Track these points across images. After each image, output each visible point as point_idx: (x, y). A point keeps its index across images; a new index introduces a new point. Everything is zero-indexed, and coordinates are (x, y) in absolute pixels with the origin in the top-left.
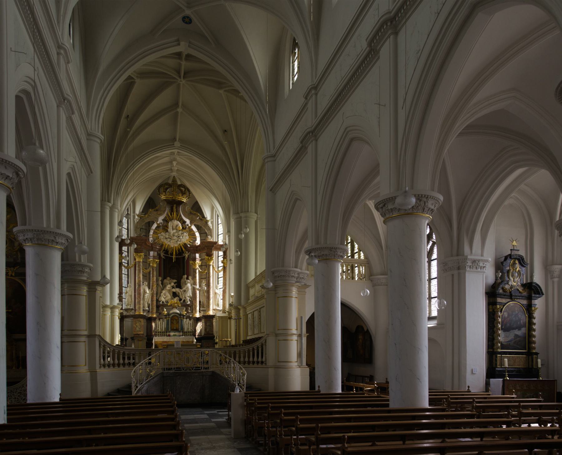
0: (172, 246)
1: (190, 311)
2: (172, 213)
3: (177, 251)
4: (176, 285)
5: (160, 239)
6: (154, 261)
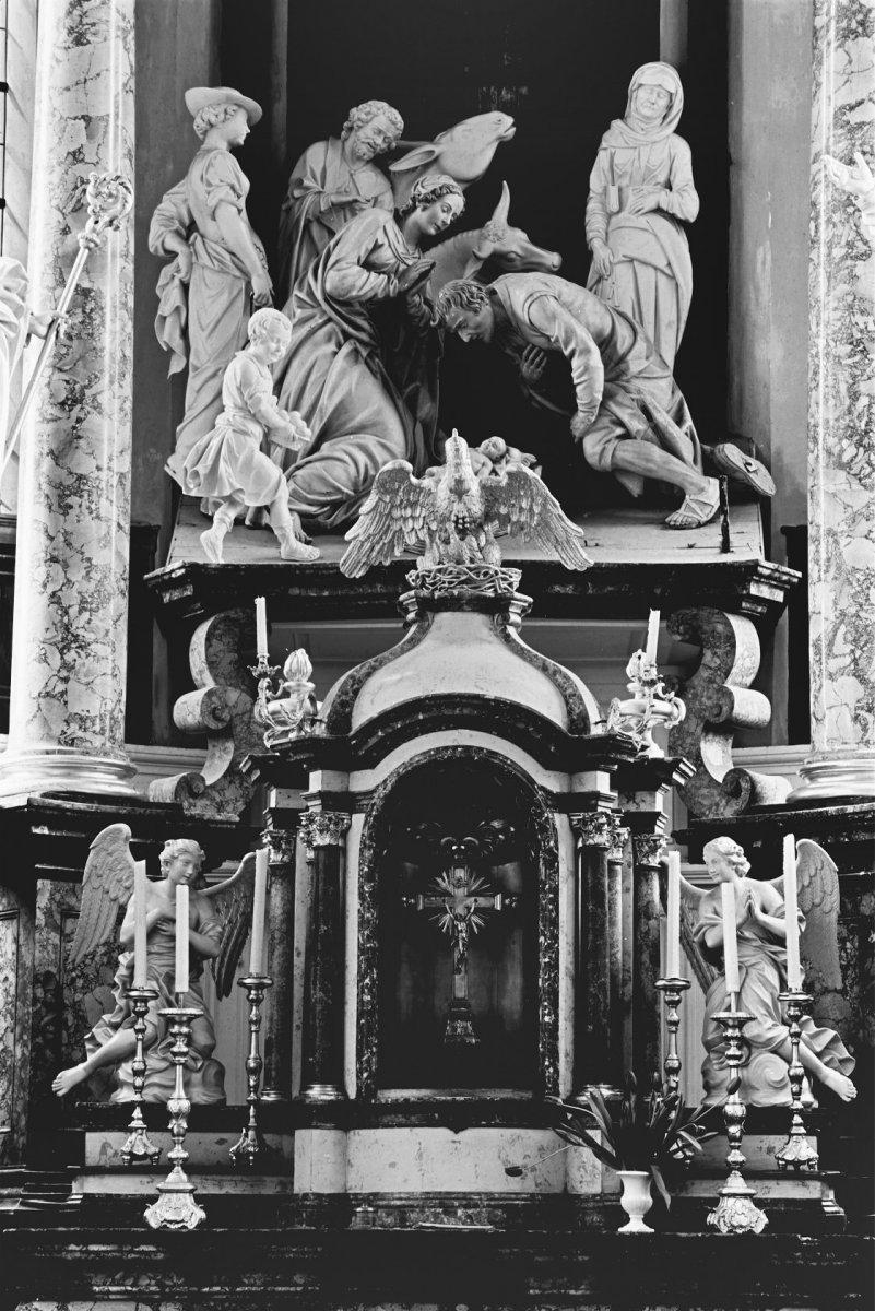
1: (753, 706)
4: (513, 221)
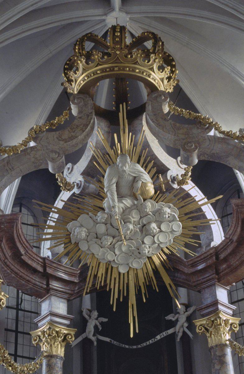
0: (122, 270)
2: (115, 135)
3: (143, 291)
5: (77, 244)
6: (52, 336)
